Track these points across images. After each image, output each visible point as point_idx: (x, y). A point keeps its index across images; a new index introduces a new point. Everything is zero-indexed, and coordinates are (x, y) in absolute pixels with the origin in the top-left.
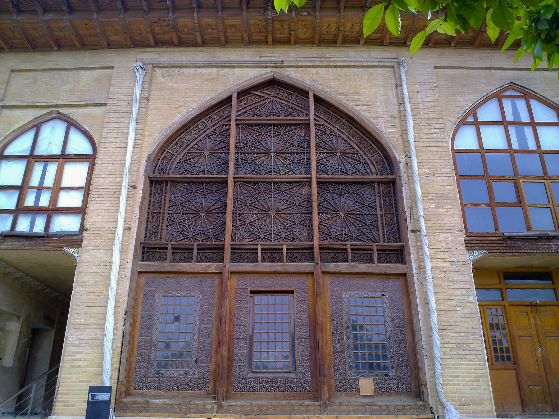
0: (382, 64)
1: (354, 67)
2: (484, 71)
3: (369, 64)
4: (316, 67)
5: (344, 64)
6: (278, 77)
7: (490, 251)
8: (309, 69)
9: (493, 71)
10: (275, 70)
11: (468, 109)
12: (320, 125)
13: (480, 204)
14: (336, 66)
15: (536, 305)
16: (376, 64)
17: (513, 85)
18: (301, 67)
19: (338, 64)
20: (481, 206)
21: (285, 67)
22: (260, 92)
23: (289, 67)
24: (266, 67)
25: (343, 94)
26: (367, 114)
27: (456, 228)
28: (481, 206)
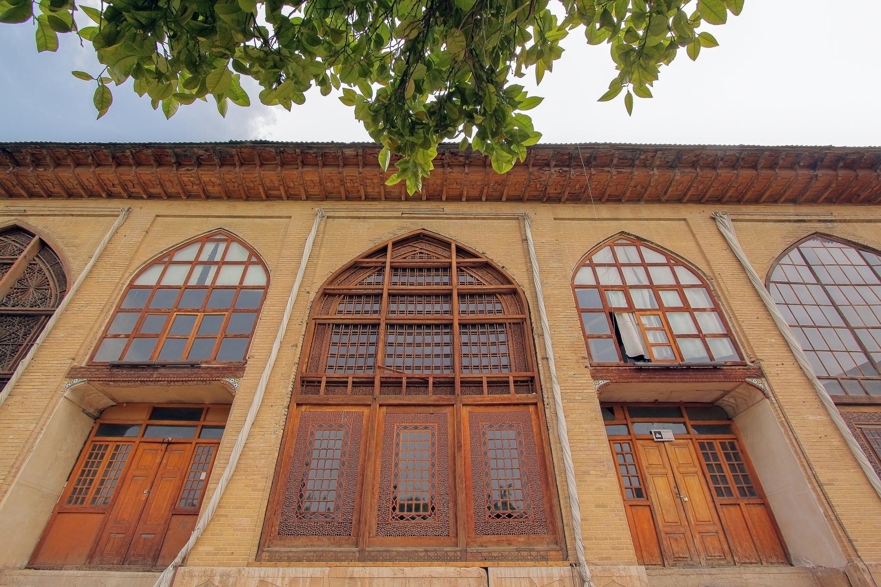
0: (112, 213)
1: (87, 215)
2: (202, 219)
3: (101, 213)
4: (55, 215)
5: (79, 213)
6: (19, 224)
7: (89, 379)
8: (48, 217)
9: (210, 219)
10: (18, 218)
11: (165, 250)
12: (34, 264)
13: (119, 335)
14: (72, 215)
15: (169, 443)
16: (106, 213)
17: (220, 231)
18: (42, 215)
19: (73, 213)
20: (121, 336)
21: (27, 215)
22: (5, 237)
23: (31, 215)
24: (12, 215)
25: (63, 238)
26: (70, 254)
27: (69, 356)
28: (121, 336)
